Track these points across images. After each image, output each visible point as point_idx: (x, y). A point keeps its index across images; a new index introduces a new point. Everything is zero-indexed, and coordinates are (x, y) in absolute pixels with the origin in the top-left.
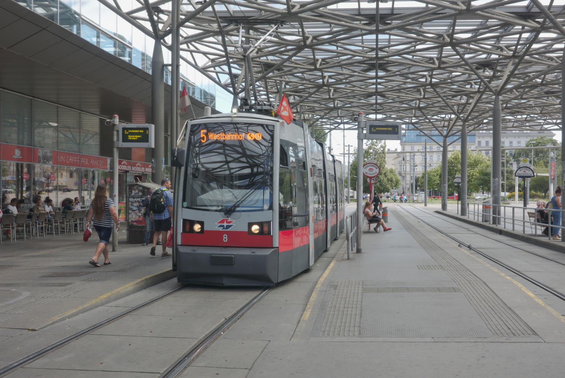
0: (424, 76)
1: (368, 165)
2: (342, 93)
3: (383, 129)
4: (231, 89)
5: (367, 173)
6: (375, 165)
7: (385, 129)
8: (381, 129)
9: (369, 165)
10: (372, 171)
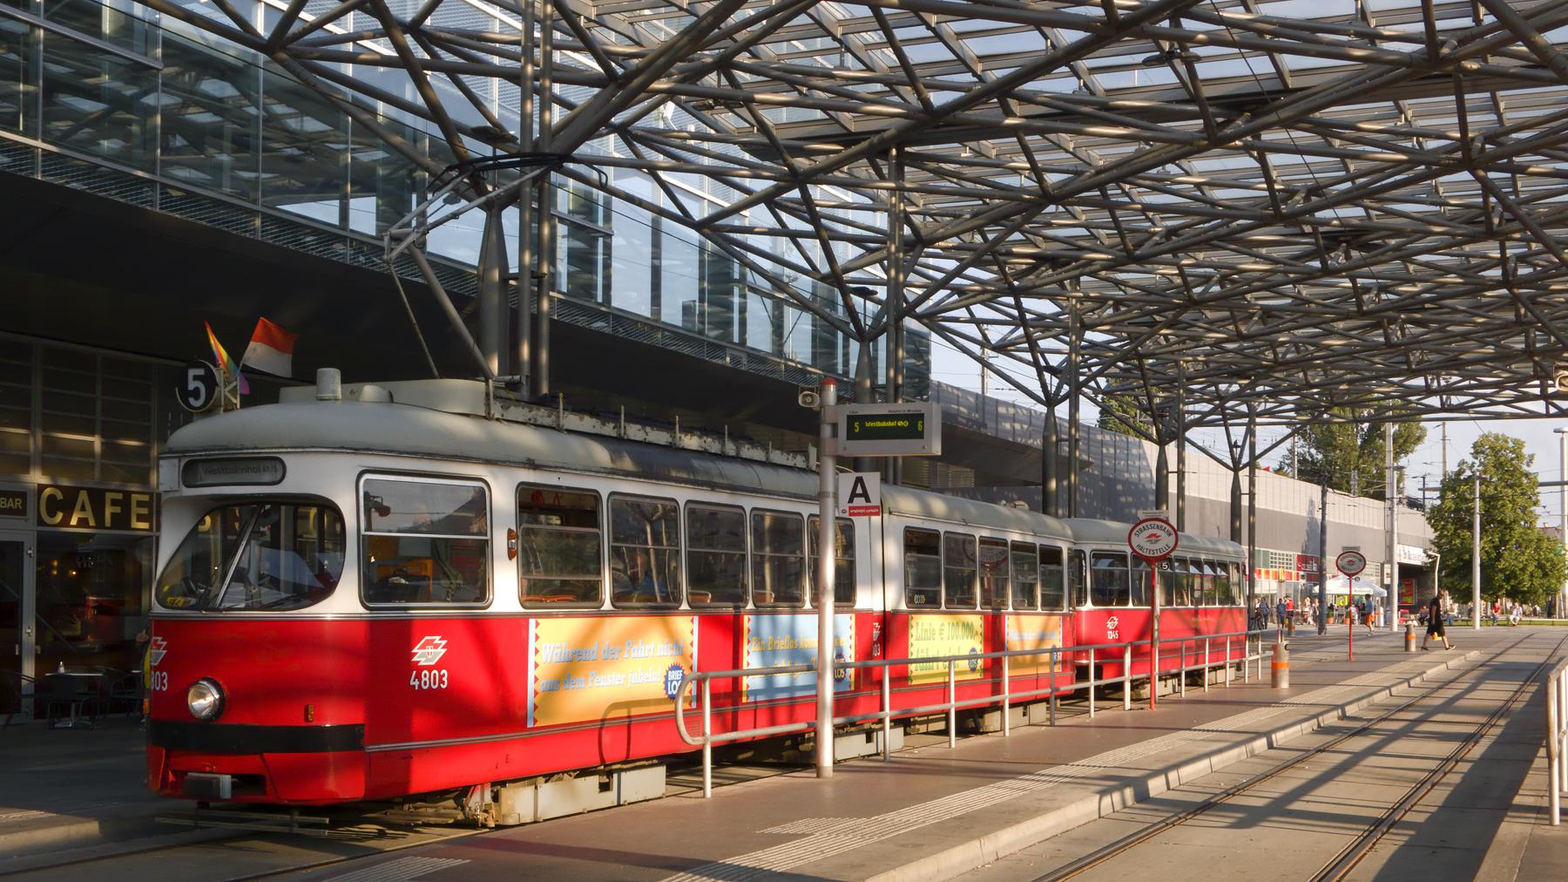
1: (1144, 524)
2: (1281, 318)
3: (884, 424)
4: (1028, 316)
5: (1141, 548)
6: (1165, 525)
7: (890, 424)
8: (879, 424)
10: (1156, 542)
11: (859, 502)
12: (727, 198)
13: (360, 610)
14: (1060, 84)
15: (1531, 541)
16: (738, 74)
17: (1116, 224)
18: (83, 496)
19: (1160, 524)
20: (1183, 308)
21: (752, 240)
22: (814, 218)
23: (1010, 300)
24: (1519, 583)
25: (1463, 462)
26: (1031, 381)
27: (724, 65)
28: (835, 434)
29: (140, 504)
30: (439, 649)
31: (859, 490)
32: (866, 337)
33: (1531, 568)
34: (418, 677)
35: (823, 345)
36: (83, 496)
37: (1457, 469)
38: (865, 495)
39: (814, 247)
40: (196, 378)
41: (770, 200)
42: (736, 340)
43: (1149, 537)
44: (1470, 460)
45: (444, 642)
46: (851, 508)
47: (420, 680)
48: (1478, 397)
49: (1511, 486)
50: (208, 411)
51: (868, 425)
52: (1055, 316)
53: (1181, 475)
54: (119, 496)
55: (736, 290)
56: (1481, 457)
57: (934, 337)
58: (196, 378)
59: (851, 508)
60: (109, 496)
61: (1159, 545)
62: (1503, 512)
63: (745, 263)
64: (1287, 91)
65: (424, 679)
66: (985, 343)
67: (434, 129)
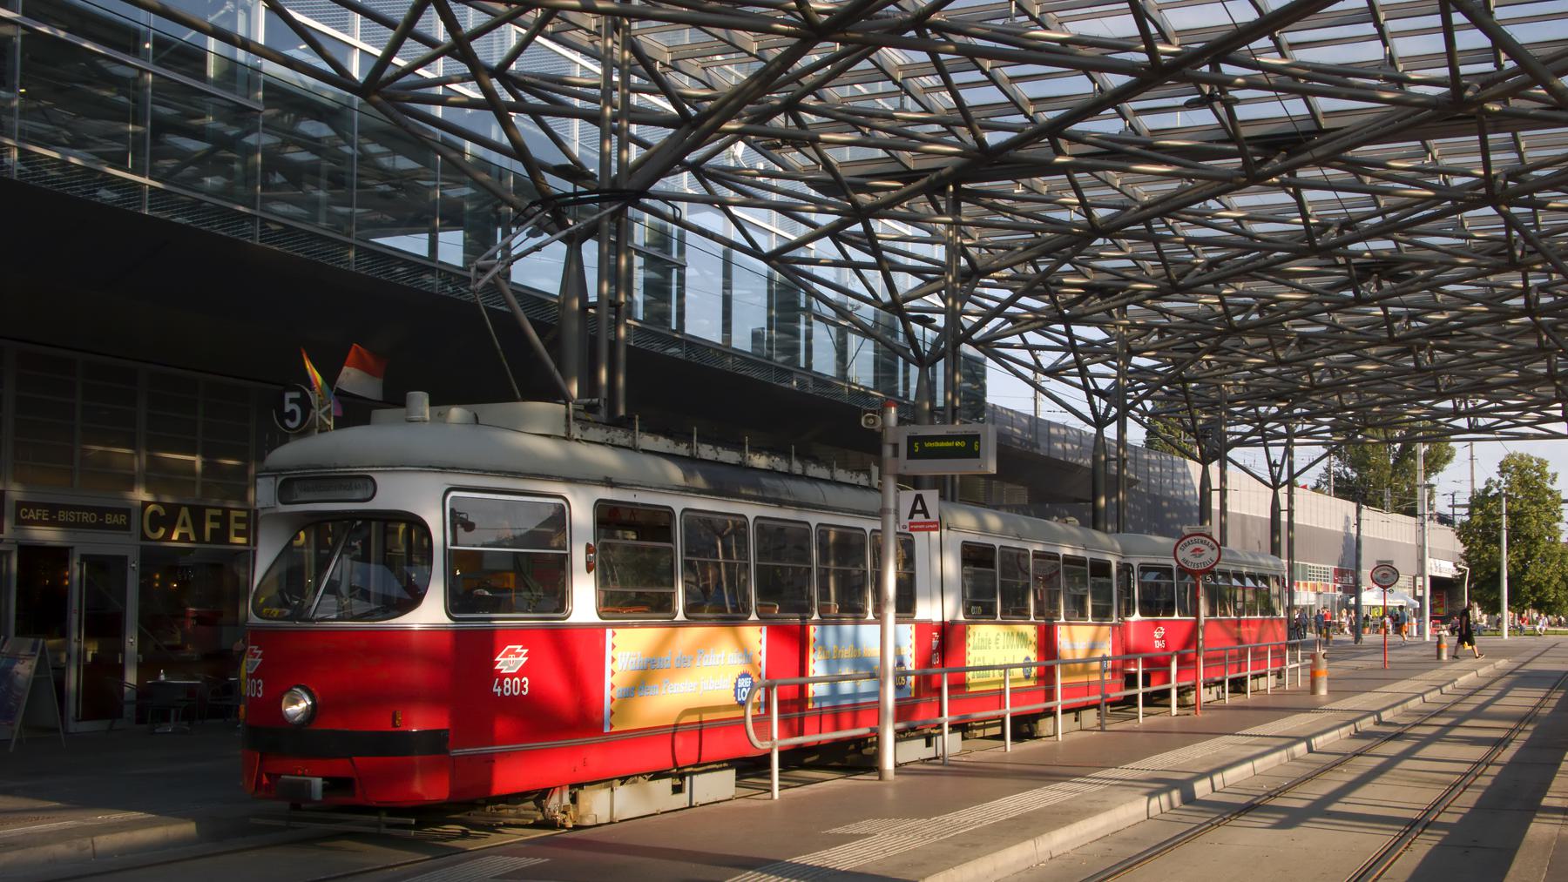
0: (1543, 289)
1: (1189, 539)
3: (942, 444)
4: (1078, 343)
5: (1186, 562)
6: (1208, 540)
8: (937, 444)
9: (1193, 538)
10: (1200, 556)
11: (919, 518)
12: (793, 231)
13: (447, 620)
14: (1108, 125)
15: (1555, 555)
16: (805, 116)
17: (1161, 256)
18: (185, 512)
19: (1204, 538)
20: (1224, 335)
21: (818, 271)
22: (876, 250)
23: (1061, 327)
24: (1545, 595)
25: (1490, 481)
26: (1078, 399)
27: (792, 107)
28: (896, 454)
29: (238, 520)
30: (521, 658)
31: (919, 507)
32: (925, 362)
33: (1555, 581)
34: (501, 684)
35: (884, 370)
36: (185, 512)
37: (1484, 487)
38: (925, 511)
39: (875, 278)
40: (292, 401)
41: (834, 233)
42: (802, 365)
43: (1194, 551)
44: (1496, 478)
45: (526, 651)
46: (911, 524)
47: (502, 687)
48: (1503, 418)
49: (1536, 503)
50: (304, 432)
51: (927, 445)
52: (1103, 343)
53: (1223, 492)
54: (219, 513)
55: (803, 318)
56: (1507, 475)
57: (990, 362)
58: (292, 401)
59: (911, 524)
60: (209, 512)
61: (1202, 559)
62: (1528, 528)
63: (811, 293)
64: (1320, 131)
65: (506, 686)
66: (1037, 368)
67: (519, 167)
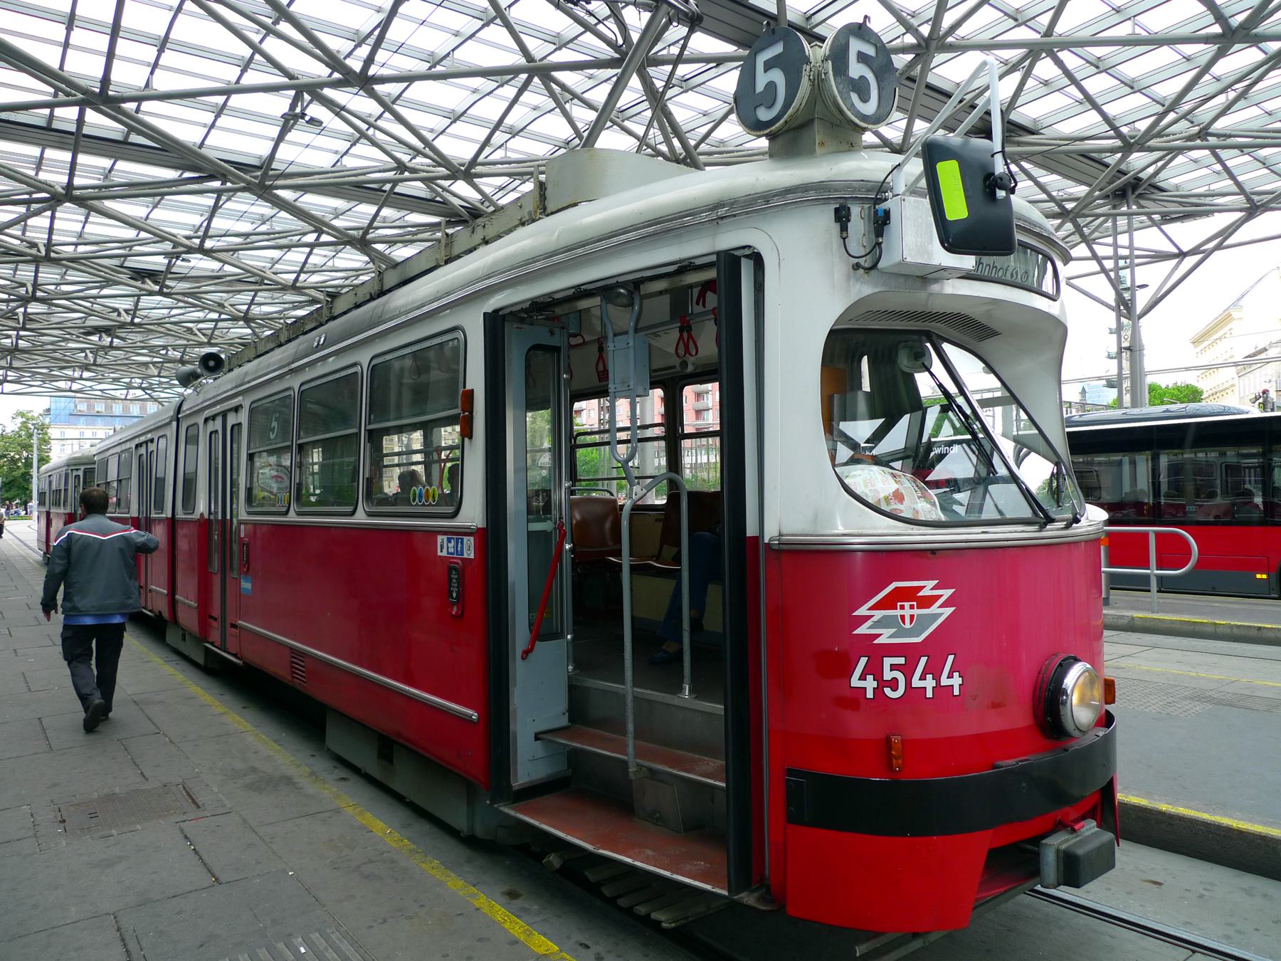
30: (934, 609)
34: (874, 669)
45: (947, 593)
47: (878, 676)
